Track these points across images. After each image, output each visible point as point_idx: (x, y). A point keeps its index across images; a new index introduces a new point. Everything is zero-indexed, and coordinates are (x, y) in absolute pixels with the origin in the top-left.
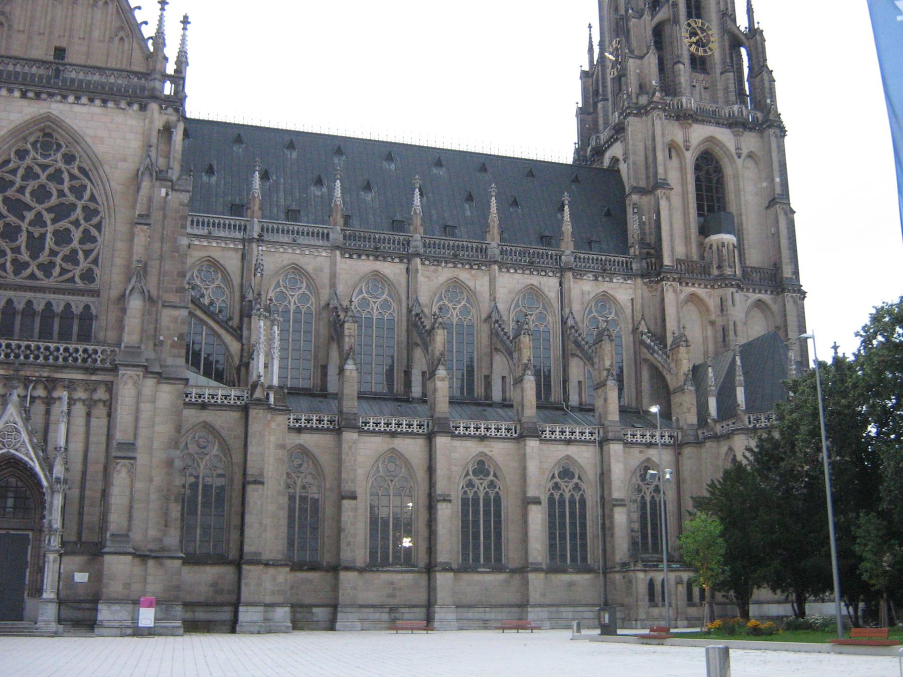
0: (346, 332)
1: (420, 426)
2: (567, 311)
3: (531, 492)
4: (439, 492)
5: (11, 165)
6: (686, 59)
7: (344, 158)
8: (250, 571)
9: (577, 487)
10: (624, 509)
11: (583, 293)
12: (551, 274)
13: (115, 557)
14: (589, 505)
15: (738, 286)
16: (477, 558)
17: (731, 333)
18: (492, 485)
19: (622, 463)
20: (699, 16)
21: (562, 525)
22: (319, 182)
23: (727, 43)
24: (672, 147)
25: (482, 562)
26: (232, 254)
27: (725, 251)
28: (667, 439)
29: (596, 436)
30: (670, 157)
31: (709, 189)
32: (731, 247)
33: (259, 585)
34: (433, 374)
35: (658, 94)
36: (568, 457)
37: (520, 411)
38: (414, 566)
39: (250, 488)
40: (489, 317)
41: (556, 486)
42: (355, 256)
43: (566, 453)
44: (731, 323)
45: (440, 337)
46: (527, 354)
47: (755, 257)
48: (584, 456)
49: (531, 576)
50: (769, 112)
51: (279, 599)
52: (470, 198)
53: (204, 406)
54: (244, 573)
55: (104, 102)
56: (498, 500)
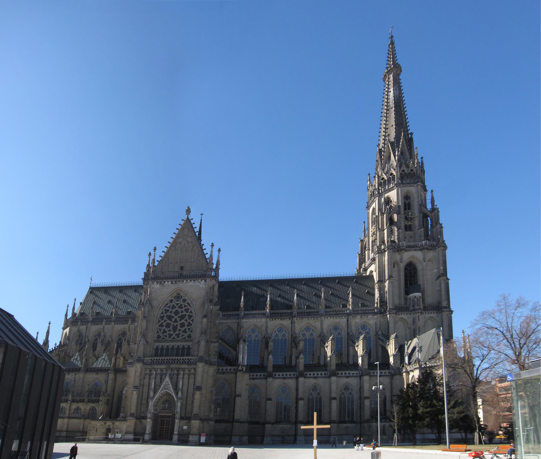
0: (270, 345)
1: (294, 375)
3: (333, 395)
5: (168, 305)
9: (350, 393)
10: (369, 400)
11: (356, 323)
14: (355, 399)
15: (421, 313)
17: (417, 331)
23: (421, 217)
27: (416, 300)
30: (394, 267)
32: (419, 298)
34: (299, 357)
36: (347, 382)
39: (237, 398)
41: (343, 393)
44: (418, 327)
45: (301, 344)
47: (430, 300)
48: (353, 382)
50: (439, 241)
53: (223, 373)
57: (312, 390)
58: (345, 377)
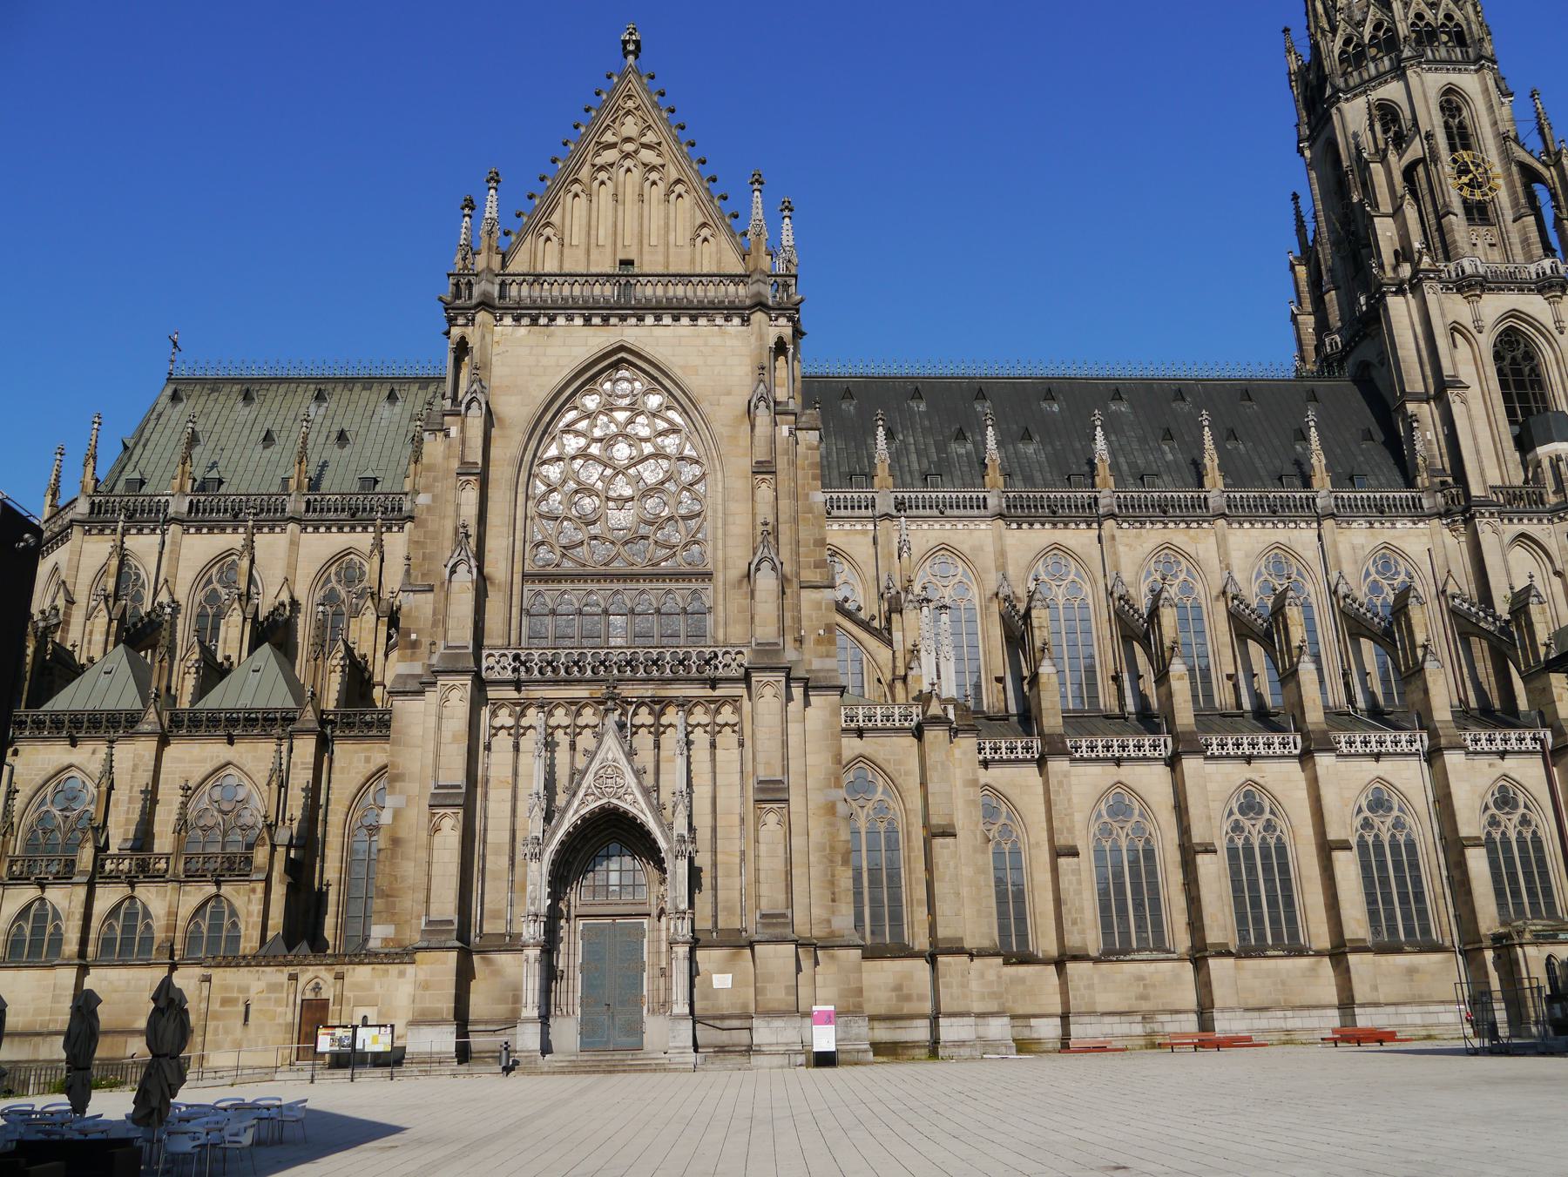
0: (1035, 623)
2: (1334, 575)
3: (1333, 834)
4: (1196, 839)
6: (1457, 206)
7: (988, 404)
8: (949, 964)
12: (1303, 525)
13: (771, 947)
14: (1421, 849)
16: (1261, 936)
18: (1269, 826)
19: (1471, 778)
20: (1467, 147)
21: (1385, 881)
22: (960, 436)
24: (1455, 329)
25: (1270, 941)
26: (859, 538)
28: (1529, 744)
29: (1417, 745)
30: (1455, 346)
31: (1520, 385)
33: (964, 985)
35: (1426, 259)
37: (1298, 715)
38: (1169, 952)
40: (1224, 593)
41: (1367, 824)
42: (1025, 526)
43: (1376, 774)
46: (1297, 634)
49: (1353, 959)
51: (993, 1006)
52: (1168, 435)
54: (941, 967)
55: (694, 318)
56: (1281, 849)
57: (1242, 811)
58: (1365, 755)
